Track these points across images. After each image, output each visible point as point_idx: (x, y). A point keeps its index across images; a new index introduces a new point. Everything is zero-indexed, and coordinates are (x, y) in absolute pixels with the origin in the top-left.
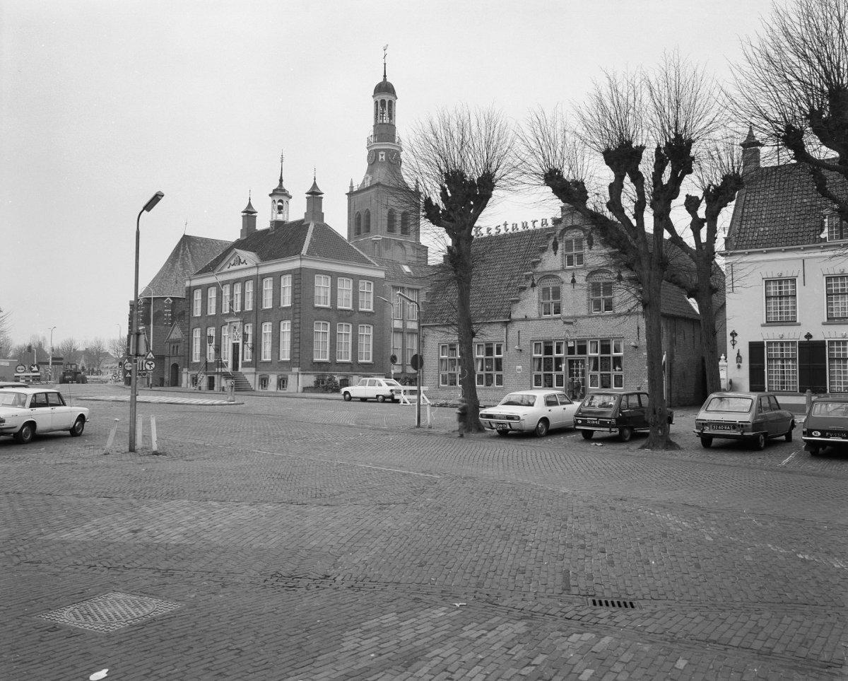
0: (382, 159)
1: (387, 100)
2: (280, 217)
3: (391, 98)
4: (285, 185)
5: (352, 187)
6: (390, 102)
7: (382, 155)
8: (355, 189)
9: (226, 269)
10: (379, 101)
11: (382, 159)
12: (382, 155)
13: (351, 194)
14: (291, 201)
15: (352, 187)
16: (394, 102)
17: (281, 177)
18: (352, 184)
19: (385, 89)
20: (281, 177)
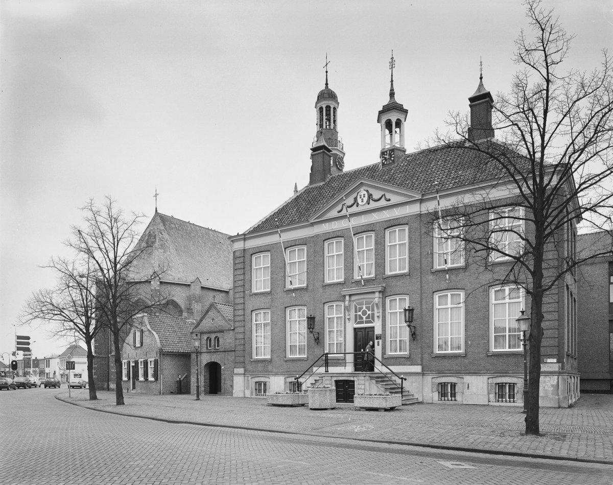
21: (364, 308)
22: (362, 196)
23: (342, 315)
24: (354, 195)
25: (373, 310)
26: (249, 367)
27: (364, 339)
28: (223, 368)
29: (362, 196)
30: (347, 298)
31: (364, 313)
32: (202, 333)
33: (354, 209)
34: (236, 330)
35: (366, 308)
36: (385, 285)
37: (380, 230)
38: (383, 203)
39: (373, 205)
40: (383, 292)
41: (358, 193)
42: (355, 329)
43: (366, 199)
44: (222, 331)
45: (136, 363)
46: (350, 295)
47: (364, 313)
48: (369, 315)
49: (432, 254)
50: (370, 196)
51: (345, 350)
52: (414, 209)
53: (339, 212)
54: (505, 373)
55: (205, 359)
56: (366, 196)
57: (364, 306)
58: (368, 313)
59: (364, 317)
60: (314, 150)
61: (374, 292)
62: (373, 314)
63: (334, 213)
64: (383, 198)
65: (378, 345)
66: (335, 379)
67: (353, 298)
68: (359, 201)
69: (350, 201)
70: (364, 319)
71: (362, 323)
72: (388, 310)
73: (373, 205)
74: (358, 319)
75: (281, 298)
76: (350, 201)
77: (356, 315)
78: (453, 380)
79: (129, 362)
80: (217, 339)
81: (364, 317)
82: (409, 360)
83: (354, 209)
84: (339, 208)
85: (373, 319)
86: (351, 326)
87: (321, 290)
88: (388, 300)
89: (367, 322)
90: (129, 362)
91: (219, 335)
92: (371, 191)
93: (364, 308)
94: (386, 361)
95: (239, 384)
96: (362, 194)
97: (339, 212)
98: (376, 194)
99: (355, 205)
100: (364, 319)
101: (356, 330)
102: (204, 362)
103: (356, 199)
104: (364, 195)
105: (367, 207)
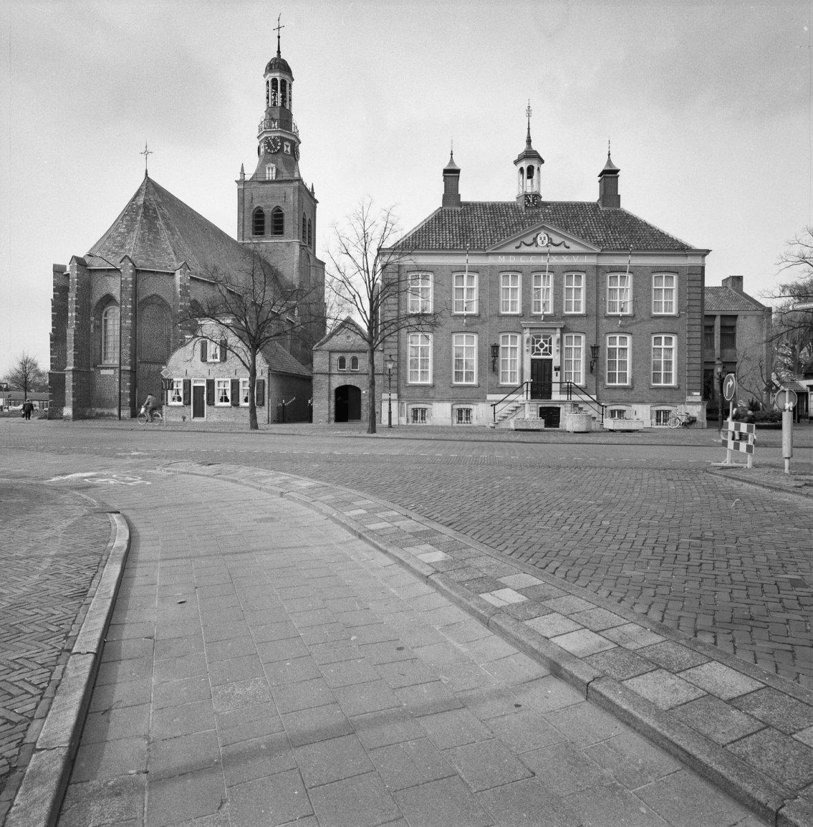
0: (287, 151)
1: (278, 79)
3: (286, 77)
4: (534, 147)
5: (243, 173)
6: (283, 82)
7: (287, 146)
8: (248, 178)
9: (511, 248)
10: (270, 80)
12: (287, 146)
13: (242, 182)
14: (543, 167)
15: (243, 173)
16: (288, 82)
19: (279, 64)
21: (542, 341)
22: (543, 239)
23: (518, 345)
24: (534, 235)
25: (550, 344)
26: (404, 393)
28: (364, 392)
29: (543, 239)
32: (331, 352)
33: (532, 249)
35: (544, 341)
36: (564, 324)
37: (561, 273)
38: (562, 249)
39: (553, 249)
40: (563, 330)
41: (538, 235)
42: (532, 360)
43: (546, 242)
46: (531, 328)
47: (542, 346)
48: (547, 348)
52: (592, 261)
53: (517, 248)
54: (663, 403)
55: (338, 381)
56: (547, 239)
58: (546, 346)
59: (542, 350)
60: (445, 171)
61: (555, 328)
62: (550, 348)
63: (511, 248)
64: (562, 245)
65: (557, 375)
66: (540, 406)
67: (533, 331)
68: (539, 242)
71: (540, 354)
72: (565, 346)
73: (553, 249)
76: (529, 240)
77: (533, 348)
78: (623, 408)
80: (355, 361)
81: (542, 350)
82: (583, 390)
83: (532, 249)
84: (517, 244)
85: (550, 352)
86: (528, 357)
89: (544, 354)
91: (357, 355)
92: (551, 236)
93: (542, 341)
95: (391, 410)
97: (517, 248)
98: (557, 240)
99: (534, 245)
101: (532, 360)
102: (335, 385)
103: (535, 239)
104: (545, 238)
105: (546, 250)
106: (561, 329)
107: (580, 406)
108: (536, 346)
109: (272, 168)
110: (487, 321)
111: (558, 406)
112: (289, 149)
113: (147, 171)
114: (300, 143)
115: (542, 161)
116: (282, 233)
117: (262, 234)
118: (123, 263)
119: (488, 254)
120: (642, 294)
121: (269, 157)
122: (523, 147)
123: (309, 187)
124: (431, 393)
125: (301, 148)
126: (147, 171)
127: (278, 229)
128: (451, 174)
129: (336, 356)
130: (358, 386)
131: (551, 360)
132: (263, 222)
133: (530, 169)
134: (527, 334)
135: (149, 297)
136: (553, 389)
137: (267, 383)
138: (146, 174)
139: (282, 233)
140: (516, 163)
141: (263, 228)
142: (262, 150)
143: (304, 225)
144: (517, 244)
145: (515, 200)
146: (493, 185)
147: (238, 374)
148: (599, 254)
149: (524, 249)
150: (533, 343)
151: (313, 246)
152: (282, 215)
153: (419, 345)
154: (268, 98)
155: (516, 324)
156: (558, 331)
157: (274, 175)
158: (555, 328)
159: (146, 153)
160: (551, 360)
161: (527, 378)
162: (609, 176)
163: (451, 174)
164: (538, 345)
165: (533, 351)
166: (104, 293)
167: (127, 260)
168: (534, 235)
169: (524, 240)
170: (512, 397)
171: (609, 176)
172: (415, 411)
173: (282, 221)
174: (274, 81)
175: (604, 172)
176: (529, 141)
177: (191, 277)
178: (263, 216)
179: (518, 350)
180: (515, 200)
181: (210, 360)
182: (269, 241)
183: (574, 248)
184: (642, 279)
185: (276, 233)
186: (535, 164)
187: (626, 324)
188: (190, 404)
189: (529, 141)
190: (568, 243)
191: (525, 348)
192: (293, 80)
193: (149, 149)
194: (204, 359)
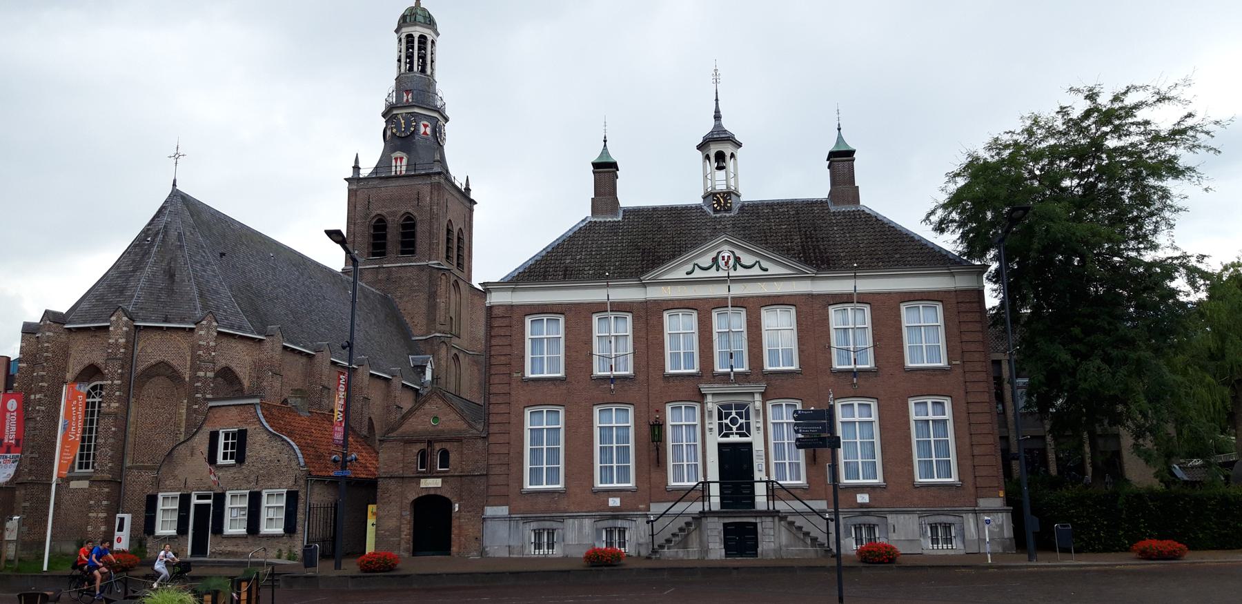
0: (425, 133)
1: (416, 36)
2: (720, 181)
4: (727, 124)
5: (356, 168)
6: (423, 38)
8: (364, 173)
9: (680, 274)
10: (403, 36)
11: (425, 133)
12: (426, 126)
13: (355, 182)
14: (739, 153)
15: (356, 168)
16: (430, 39)
17: (717, 112)
18: (357, 160)
20: (717, 112)
21: (734, 415)
23: (698, 422)
25: (748, 418)
27: (736, 462)
30: (709, 398)
31: (734, 421)
34: (491, 439)
37: (753, 307)
38: (756, 271)
39: (741, 272)
40: (765, 397)
42: (720, 445)
43: (731, 262)
44: (459, 440)
45: (220, 499)
46: (713, 394)
47: (734, 421)
49: (830, 347)
50: (737, 260)
51: (705, 476)
57: (734, 412)
59: (734, 428)
61: (752, 394)
62: (748, 425)
63: (680, 274)
68: (722, 263)
69: (706, 261)
70: (734, 430)
73: (741, 272)
74: (724, 430)
75: (579, 389)
76: (706, 261)
77: (720, 425)
79: (189, 496)
80: (445, 455)
81: (734, 428)
83: (712, 273)
85: (748, 430)
86: (714, 440)
87: (662, 383)
88: (769, 405)
90: (185, 500)
91: (447, 446)
92: (738, 253)
93: (734, 415)
94: (773, 492)
96: (726, 255)
98: (747, 259)
100: (734, 430)
101: (720, 445)
106: (762, 394)
107: (790, 519)
108: (724, 421)
109: (401, 159)
110: (649, 388)
111: (753, 520)
112: (428, 130)
113: (175, 181)
114: (447, 120)
115: (739, 145)
116: (413, 252)
117: (383, 254)
118: (113, 318)
119: (644, 285)
120: (887, 334)
121: (398, 142)
122: (708, 126)
123: (460, 182)
124: (563, 504)
125: (449, 129)
126: (175, 181)
127: (408, 245)
128: (605, 170)
129: (416, 449)
130: (447, 496)
131: (750, 444)
132: (384, 237)
133: (720, 157)
134: (712, 404)
135: (153, 366)
136: (757, 492)
137: (302, 495)
138: (174, 185)
139: (413, 252)
140: (700, 147)
141: (384, 246)
142: (389, 133)
143: (448, 240)
144: (689, 267)
145: (700, 201)
146: (663, 179)
147: (261, 483)
148: (813, 278)
149: (698, 274)
150: (720, 418)
151: (466, 270)
152: (413, 226)
153: (541, 427)
154: (399, 60)
155: (690, 389)
156: (758, 397)
157: (404, 168)
158: (752, 394)
159: (177, 156)
160: (750, 444)
161: (714, 473)
162: (841, 159)
163: (605, 170)
164: (728, 421)
165: (720, 431)
166: (87, 362)
167: (120, 312)
168: (714, 254)
169: (698, 261)
170: (680, 507)
171: (841, 159)
172: (538, 533)
173: (413, 235)
174: (410, 38)
175: (832, 155)
176: (717, 117)
177: (219, 333)
178: (385, 228)
179: (698, 429)
180: (700, 201)
181: (220, 460)
182: (392, 264)
183: (774, 270)
184: (886, 312)
185: (403, 252)
186: (728, 149)
187: (854, 383)
188: (187, 533)
189: (717, 117)
190: (764, 264)
191: (707, 426)
192: (438, 35)
193: (181, 151)
194: (212, 459)
